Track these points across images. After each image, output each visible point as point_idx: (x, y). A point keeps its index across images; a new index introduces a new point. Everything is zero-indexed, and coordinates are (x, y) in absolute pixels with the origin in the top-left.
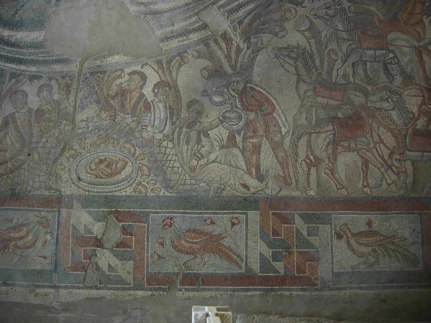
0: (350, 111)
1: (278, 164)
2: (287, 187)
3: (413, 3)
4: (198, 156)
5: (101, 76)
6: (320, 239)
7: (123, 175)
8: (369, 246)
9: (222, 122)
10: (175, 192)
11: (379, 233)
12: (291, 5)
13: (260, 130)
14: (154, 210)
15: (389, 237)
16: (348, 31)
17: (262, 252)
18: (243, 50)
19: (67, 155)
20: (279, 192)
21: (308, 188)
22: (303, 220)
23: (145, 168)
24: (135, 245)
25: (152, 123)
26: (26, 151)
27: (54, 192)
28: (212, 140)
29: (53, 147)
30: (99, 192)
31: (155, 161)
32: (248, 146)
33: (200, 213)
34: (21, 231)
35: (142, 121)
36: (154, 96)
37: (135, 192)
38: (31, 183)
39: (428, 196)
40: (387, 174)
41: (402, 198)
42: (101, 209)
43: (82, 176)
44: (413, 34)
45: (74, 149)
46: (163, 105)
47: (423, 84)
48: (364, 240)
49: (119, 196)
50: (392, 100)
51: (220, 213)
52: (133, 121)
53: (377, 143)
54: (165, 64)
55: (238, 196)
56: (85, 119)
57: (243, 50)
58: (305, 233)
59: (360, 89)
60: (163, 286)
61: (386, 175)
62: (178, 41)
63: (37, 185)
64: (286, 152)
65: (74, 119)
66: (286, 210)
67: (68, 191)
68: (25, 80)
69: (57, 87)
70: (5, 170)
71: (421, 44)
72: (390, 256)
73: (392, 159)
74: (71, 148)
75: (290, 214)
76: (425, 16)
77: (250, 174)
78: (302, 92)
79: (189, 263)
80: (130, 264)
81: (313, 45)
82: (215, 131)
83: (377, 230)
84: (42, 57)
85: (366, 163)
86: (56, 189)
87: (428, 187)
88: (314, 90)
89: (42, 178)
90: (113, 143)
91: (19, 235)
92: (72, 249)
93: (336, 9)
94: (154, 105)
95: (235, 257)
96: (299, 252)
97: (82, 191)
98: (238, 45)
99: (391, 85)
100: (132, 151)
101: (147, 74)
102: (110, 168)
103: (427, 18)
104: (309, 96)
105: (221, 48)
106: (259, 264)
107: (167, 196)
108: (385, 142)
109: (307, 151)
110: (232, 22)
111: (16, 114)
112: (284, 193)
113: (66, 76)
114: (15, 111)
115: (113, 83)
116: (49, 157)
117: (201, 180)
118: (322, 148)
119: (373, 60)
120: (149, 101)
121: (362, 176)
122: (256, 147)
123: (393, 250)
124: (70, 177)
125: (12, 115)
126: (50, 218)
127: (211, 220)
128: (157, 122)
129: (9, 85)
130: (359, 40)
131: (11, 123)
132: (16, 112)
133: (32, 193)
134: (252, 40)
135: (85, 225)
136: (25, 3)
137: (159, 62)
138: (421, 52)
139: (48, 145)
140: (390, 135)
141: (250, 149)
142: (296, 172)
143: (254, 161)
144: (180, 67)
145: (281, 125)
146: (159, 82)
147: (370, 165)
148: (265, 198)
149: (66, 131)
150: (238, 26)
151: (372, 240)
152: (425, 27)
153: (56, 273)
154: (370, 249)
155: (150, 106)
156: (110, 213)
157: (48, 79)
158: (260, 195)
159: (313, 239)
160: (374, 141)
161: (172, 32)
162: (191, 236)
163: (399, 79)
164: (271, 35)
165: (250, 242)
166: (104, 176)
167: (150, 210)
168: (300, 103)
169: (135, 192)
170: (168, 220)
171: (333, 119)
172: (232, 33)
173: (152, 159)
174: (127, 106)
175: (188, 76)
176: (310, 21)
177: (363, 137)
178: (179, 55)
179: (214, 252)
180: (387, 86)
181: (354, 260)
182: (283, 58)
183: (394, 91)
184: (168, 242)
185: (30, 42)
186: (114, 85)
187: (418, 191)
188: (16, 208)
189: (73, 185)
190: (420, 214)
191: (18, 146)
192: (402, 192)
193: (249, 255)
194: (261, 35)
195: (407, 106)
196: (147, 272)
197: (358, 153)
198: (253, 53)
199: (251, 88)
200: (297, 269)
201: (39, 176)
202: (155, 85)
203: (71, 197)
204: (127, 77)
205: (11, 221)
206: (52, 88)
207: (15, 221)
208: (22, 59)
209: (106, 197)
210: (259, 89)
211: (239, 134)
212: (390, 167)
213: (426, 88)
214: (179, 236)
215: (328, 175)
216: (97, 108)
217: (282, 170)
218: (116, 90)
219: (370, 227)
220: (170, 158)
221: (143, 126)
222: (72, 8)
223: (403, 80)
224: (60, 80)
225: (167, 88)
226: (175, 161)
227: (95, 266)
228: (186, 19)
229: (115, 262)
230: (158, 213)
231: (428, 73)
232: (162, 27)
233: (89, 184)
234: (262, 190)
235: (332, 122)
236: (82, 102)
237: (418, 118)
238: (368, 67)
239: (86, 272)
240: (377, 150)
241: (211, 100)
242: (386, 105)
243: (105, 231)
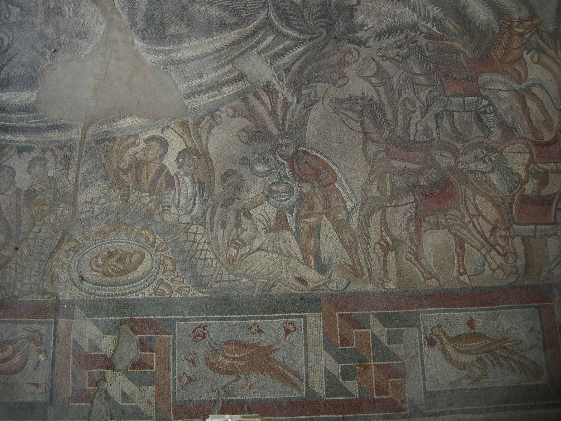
0: (435, 176)
1: (344, 249)
2: (358, 279)
3: (509, 35)
4: (238, 243)
5: (110, 145)
6: (405, 347)
7: (140, 271)
8: (473, 354)
9: (268, 197)
10: (209, 291)
11: (484, 335)
12: (351, 46)
13: (319, 206)
14: (182, 317)
15: (499, 341)
16: (427, 74)
17: (328, 367)
18: (291, 104)
19: (66, 248)
20: (347, 286)
21: (385, 280)
22: (380, 322)
23: (168, 262)
24: (157, 365)
25: (177, 203)
26: (13, 244)
28: (256, 221)
29: (47, 238)
30: (109, 295)
31: (182, 251)
32: (303, 228)
33: (243, 319)
35: (163, 201)
36: (179, 168)
37: (155, 293)
38: (19, 286)
39: (546, 282)
40: (490, 257)
41: (512, 287)
42: (110, 318)
43: (86, 275)
44: (511, 74)
45: (75, 239)
46: (190, 179)
47: (530, 137)
48: (465, 346)
49: (135, 299)
50: (492, 161)
51: (269, 318)
52: (152, 200)
53: (474, 216)
54: (191, 127)
55: (292, 294)
56: (90, 200)
57: (291, 104)
58: (384, 340)
59: (447, 147)
60: (196, 418)
61: (488, 258)
62: (208, 97)
63: (26, 288)
64: (354, 234)
65: (74, 201)
66: (358, 310)
67: (68, 294)
68: (12, 153)
69: (53, 160)
71: (523, 86)
72: (501, 367)
73: (495, 235)
74: (71, 239)
75: (363, 315)
76: (526, 52)
77: (307, 263)
78: (371, 155)
79: (230, 386)
80: (151, 391)
81: (382, 93)
82: (259, 209)
83: (481, 331)
84: (33, 123)
85: (461, 243)
86: (52, 293)
87: (545, 271)
88: (387, 150)
89: (33, 280)
90: (126, 230)
91: (3, 356)
92: (73, 373)
93: (409, 48)
94: (178, 179)
95: (292, 376)
96: (378, 366)
97: (85, 294)
98: (286, 98)
99: (487, 140)
100: (151, 239)
101: (169, 140)
102: (122, 263)
103: (528, 53)
104: (380, 159)
105: (263, 103)
106: (324, 383)
107: (198, 297)
108: (485, 214)
109: (382, 231)
110: (277, 70)
112: (354, 287)
113: (65, 146)
115: (125, 152)
116: (43, 251)
117: (244, 275)
118: (401, 226)
119: (462, 109)
120: (172, 173)
121: (456, 260)
122: (313, 229)
123: (505, 358)
124: (70, 277)
126: (43, 329)
127: (258, 327)
128: (183, 201)
130: (442, 85)
133: (21, 299)
134: (304, 92)
135: (90, 340)
137: (184, 124)
138: (524, 96)
139: (42, 235)
140: (490, 204)
141: (306, 232)
142: (368, 258)
143: (312, 246)
144: (211, 130)
145: (345, 199)
146: (185, 149)
147: (466, 245)
148: (329, 295)
150: (284, 74)
151: (476, 346)
152: (526, 65)
153: (51, 405)
154: (474, 358)
155: (173, 180)
156: (123, 322)
157: (41, 150)
158: (322, 292)
159: (396, 348)
160: (469, 214)
161: (200, 85)
162: (232, 349)
163: (497, 133)
164: (327, 85)
165: (310, 355)
166: (114, 274)
167: (176, 317)
168: (369, 169)
169: (155, 293)
170: (200, 329)
171: (414, 188)
172: (277, 85)
173: (178, 249)
174: (144, 181)
175: (222, 141)
176: (377, 64)
177: (454, 209)
178: (210, 114)
179: (263, 370)
180: (483, 141)
181: (453, 374)
182: (344, 112)
183: (492, 147)
184: (201, 360)
185: (18, 105)
186: (126, 155)
187: (533, 277)
189: (74, 287)
190: (538, 307)
192: (512, 279)
193: (310, 372)
194: (314, 84)
195: (510, 166)
196: (174, 400)
197: (449, 230)
198: (305, 107)
199: (304, 152)
200: (376, 389)
201: (30, 276)
202: (180, 153)
203: (71, 303)
204: (143, 145)
208: (8, 126)
209: (118, 302)
210: (314, 153)
211: (291, 212)
212: (493, 247)
213: (534, 142)
214: (216, 350)
215: (411, 261)
216: (105, 186)
217: (350, 257)
218: (129, 161)
219: (472, 328)
220: (200, 247)
221: (164, 206)
222: (72, 60)
223: (502, 133)
224: (57, 151)
225: (195, 157)
226: (207, 250)
227: (104, 395)
228: (217, 69)
229: (131, 388)
230: (186, 320)
231: (534, 123)
232: (186, 79)
233: (95, 284)
234: (324, 284)
235: (413, 192)
236: (86, 178)
237: (526, 182)
238: (455, 118)
239: (92, 403)
240: (474, 225)
241: (252, 169)
242: (482, 166)
243: (117, 346)
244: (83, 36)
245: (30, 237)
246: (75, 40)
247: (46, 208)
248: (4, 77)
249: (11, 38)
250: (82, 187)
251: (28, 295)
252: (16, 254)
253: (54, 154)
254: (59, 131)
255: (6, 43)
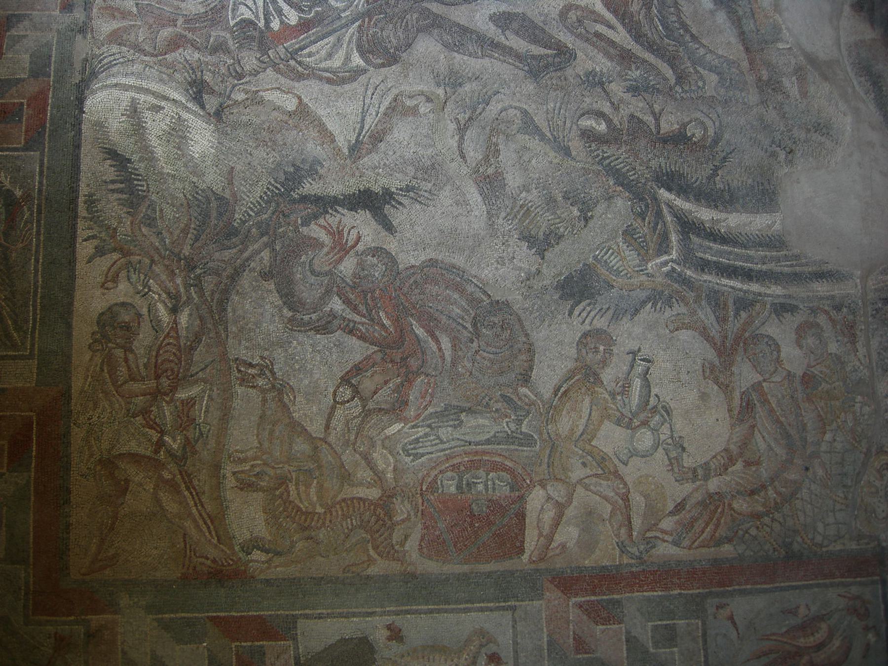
27: (868, 544)
34: (817, 631)
38: (820, 527)
70: (764, 505)
84: (787, 266)
111: (764, 384)
114: (761, 379)
125: (757, 387)
129: (738, 325)
131: (758, 405)
132: (764, 380)
136: (728, 154)
149: (866, 417)
188: (800, 583)
191: (781, 451)
205: (794, 612)
206: (822, 329)
207: (802, 611)
208: (750, 270)
244: (824, 130)
245: (822, 449)
246: (816, 137)
247: (837, 403)
248: (722, 187)
249: (717, 124)
250: (880, 370)
251: (835, 541)
252: (807, 477)
253: (830, 318)
254: (828, 281)
255: (711, 132)
